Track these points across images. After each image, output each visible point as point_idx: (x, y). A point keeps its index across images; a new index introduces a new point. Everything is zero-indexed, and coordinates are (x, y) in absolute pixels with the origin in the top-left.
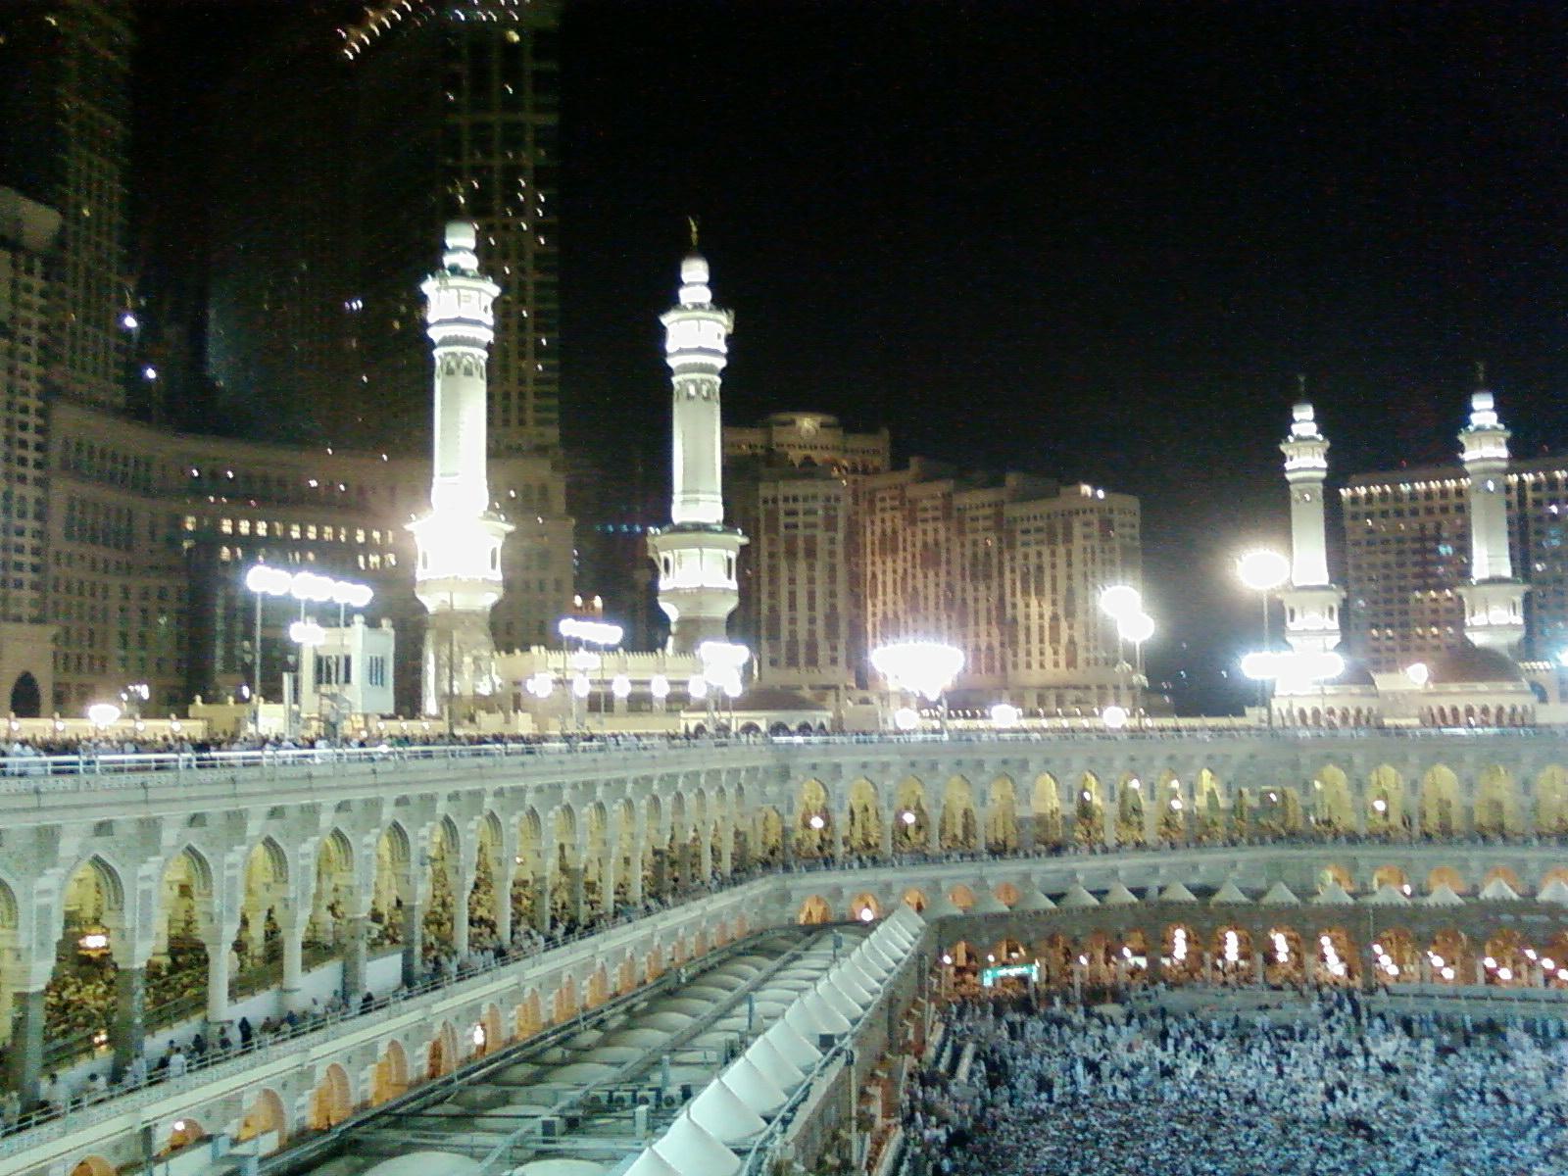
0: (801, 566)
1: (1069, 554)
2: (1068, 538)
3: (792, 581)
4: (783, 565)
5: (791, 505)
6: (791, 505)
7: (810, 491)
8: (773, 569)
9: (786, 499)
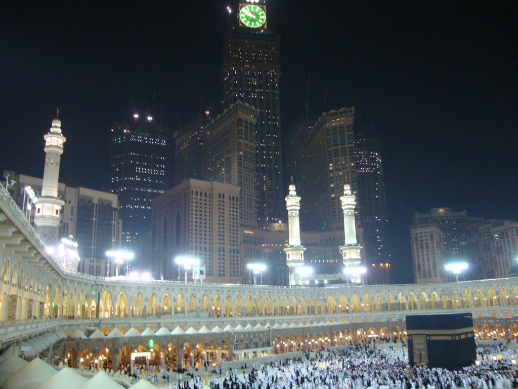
0: (425, 250)
1: (508, 241)
2: (507, 237)
3: (423, 255)
4: (420, 251)
5: (421, 235)
6: (421, 235)
7: (426, 231)
8: (418, 253)
9: (419, 233)
